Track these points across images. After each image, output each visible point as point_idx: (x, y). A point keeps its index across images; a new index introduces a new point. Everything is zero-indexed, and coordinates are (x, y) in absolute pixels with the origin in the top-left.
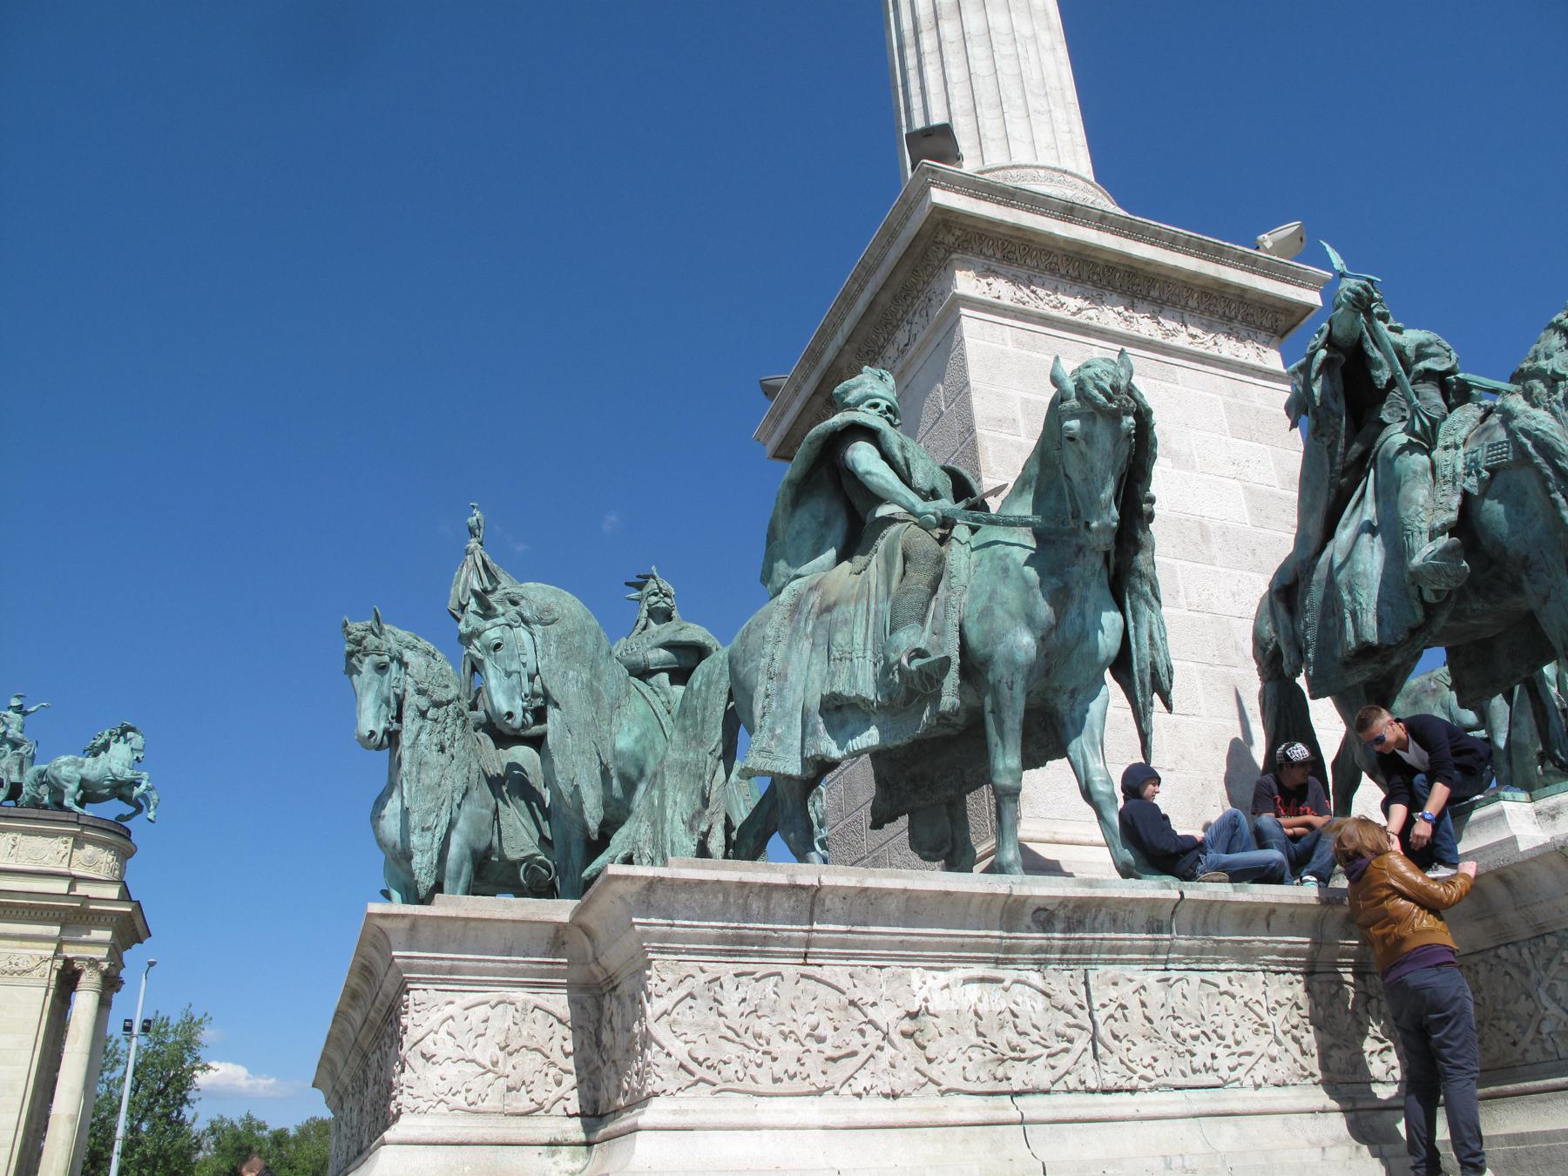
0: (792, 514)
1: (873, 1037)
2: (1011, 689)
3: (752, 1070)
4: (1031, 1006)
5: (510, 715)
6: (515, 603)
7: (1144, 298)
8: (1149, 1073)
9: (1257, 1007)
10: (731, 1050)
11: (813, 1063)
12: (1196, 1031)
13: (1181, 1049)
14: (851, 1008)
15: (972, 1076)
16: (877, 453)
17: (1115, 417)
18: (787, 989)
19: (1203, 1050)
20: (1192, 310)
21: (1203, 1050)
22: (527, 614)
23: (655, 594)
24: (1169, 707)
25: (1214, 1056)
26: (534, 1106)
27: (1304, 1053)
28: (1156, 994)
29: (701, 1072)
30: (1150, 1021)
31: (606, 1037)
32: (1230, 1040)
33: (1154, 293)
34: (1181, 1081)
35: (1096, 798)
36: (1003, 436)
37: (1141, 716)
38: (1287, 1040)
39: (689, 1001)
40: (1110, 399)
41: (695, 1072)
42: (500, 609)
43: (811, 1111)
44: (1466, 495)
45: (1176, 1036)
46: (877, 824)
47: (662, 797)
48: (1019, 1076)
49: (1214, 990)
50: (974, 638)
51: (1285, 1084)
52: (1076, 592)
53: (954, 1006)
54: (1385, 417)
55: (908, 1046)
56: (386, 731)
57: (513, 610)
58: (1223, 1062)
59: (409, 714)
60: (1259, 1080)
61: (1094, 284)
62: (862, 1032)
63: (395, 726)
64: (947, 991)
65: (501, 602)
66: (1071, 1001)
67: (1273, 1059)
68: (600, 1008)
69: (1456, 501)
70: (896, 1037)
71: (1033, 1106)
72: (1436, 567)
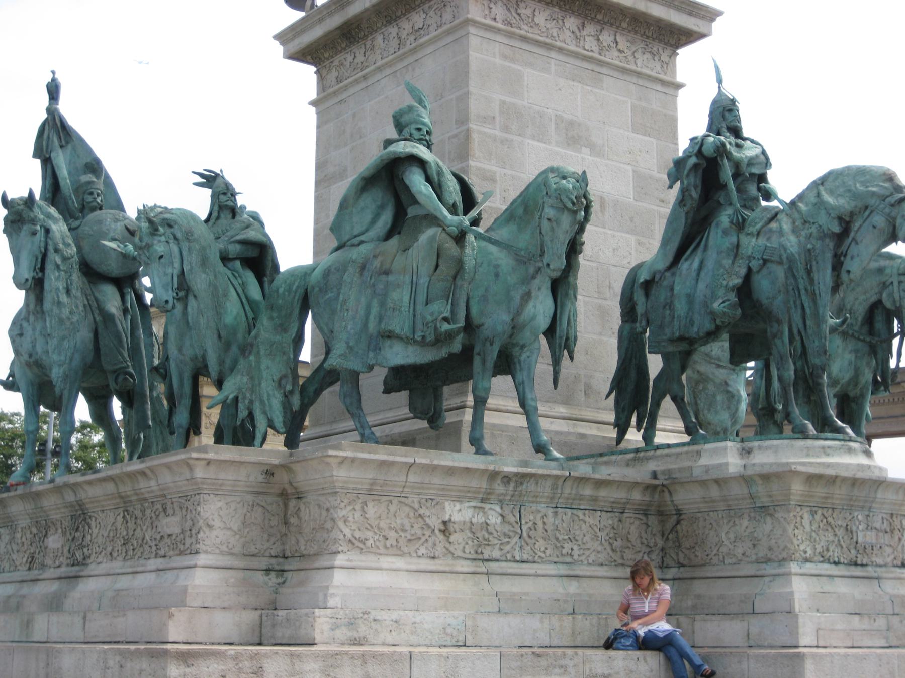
0: (361, 194)
1: (428, 533)
2: (491, 344)
3: (377, 543)
4: (494, 519)
5: (167, 302)
6: (170, 226)
7: (592, 19)
8: (543, 555)
9: (595, 528)
10: (369, 534)
11: (402, 542)
12: (566, 537)
13: (558, 545)
14: (420, 519)
15: (467, 551)
16: (424, 176)
17: (575, 213)
18: (393, 508)
19: (567, 546)
20: (624, 29)
21: (567, 546)
22: (179, 235)
23: (225, 194)
24: (572, 358)
25: (572, 549)
26: (257, 551)
27: (613, 550)
28: (550, 519)
29: (357, 544)
30: (546, 531)
31: (293, 520)
32: (580, 543)
33: (599, 17)
34: (556, 560)
35: (527, 408)
36: (486, 130)
37: (556, 362)
38: (606, 545)
39: (353, 512)
40: (573, 204)
41: (357, 544)
42: (161, 229)
43: (399, 563)
44: (750, 270)
45: (557, 539)
46: (387, 391)
47: (258, 362)
48: (487, 553)
49: (576, 518)
50: (474, 311)
51: (602, 565)
52: (533, 295)
53: (462, 519)
54: (722, 200)
55: (441, 537)
56: (34, 278)
57: (169, 231)
58: (576, 553)
59: (49, 267)
60: (591, 561)
61: (560, 7)
62: (423, 528)
63: (40, 275)
64: (459, 513)
65: (163, 226)
66: (512, 520)
67: (598, 552)
68: (286, 506)
69: (743, 271)
70: (437, 532)
71: (494, 566)
72: (724, 313)
